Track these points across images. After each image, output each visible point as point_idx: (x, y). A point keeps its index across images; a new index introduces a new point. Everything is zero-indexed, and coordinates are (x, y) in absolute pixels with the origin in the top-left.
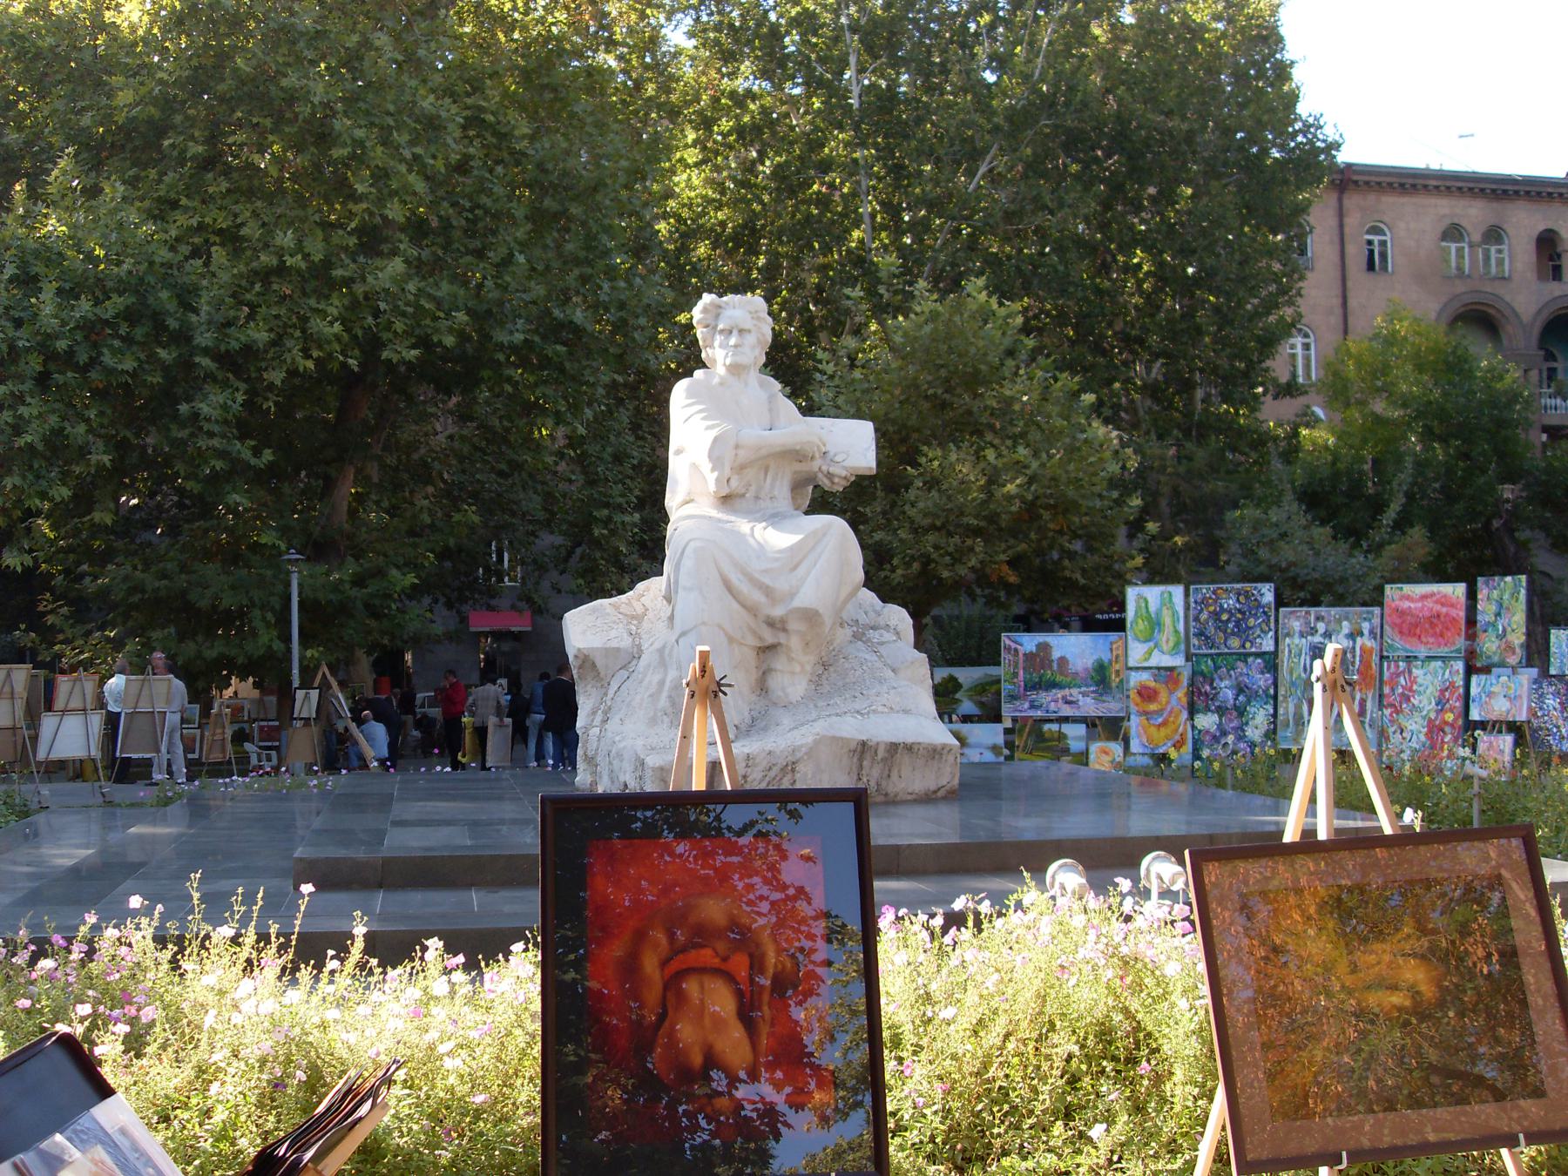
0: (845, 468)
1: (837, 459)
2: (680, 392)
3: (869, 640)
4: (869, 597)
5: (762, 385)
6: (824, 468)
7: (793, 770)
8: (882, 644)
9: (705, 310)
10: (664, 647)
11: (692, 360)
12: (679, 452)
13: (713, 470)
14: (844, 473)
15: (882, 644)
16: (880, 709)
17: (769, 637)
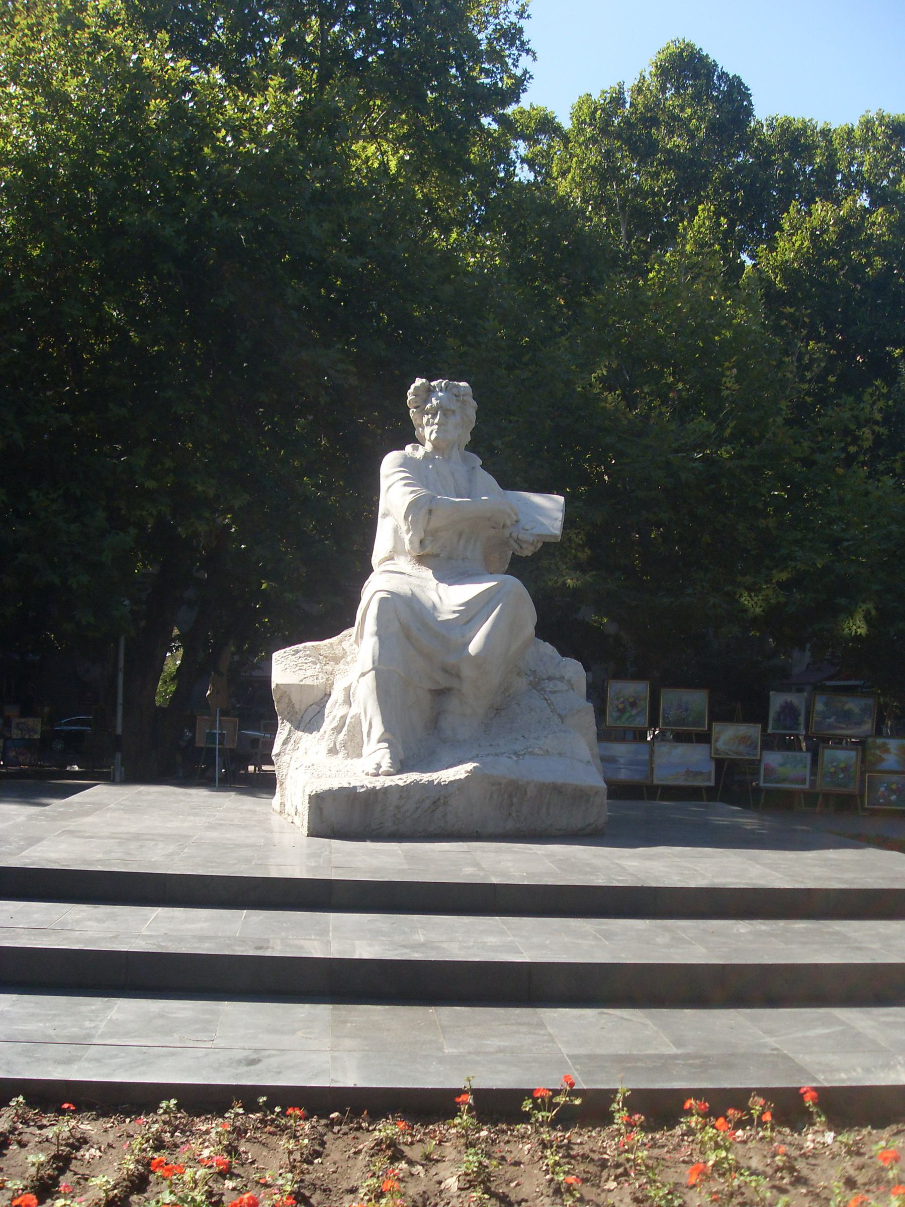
0: (532, 535)
1: (527, 527)
2: (390, 465)
3: (543, 689)
4: (548, 649)
5: (465, 460)
6: (515, 535)
7: (445, 803)
8: (555, 692)
9: (415, 394)
10: (350, 686)
11: (406, 435)
12: (385, 515)
13: (408, 531)
14: (531, 539)
15: (555, 692)
16: (537, 751)
17: (443, 682)
